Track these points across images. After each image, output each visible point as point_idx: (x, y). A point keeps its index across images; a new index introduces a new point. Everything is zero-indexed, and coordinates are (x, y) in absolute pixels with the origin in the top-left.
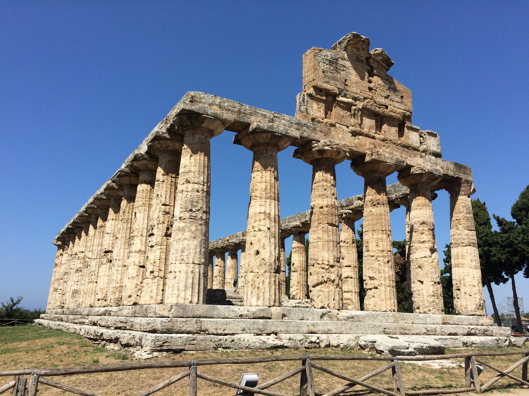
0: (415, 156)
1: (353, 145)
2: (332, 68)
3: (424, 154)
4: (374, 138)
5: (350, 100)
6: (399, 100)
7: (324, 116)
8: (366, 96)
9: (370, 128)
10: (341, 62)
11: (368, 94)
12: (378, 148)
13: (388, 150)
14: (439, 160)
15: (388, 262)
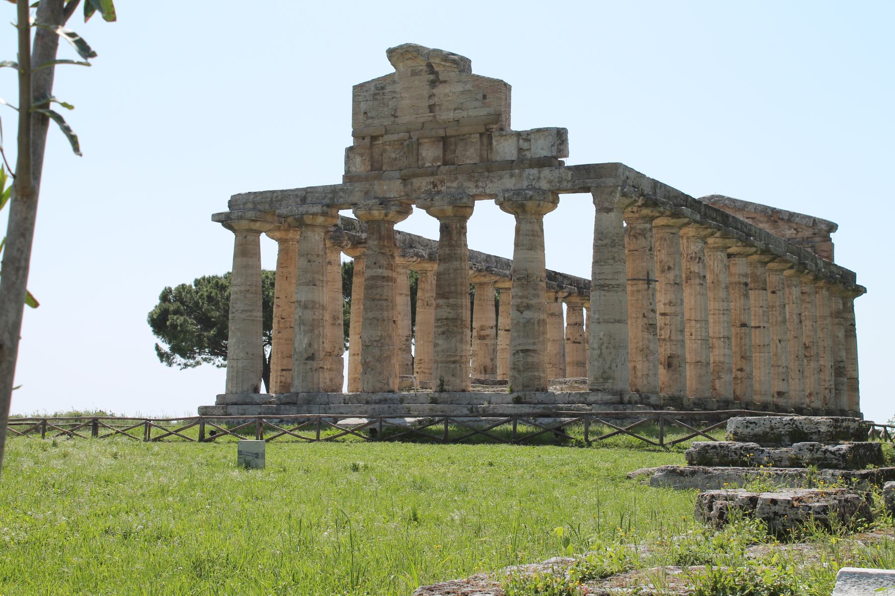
0: (501, 178)
1: (403, 194)
2: (376, 103)
3: (517, 171)
4: (433, 174)
5: (402, 135)
6: (478, 104)
7: (369, 168)
8: (422, 120)
9: (435, 159)
10: (389, 89)
11: (427, 116)
12: (440, 187)
13: (455, 184)
14: (546, 172)
15: (443, 333)
